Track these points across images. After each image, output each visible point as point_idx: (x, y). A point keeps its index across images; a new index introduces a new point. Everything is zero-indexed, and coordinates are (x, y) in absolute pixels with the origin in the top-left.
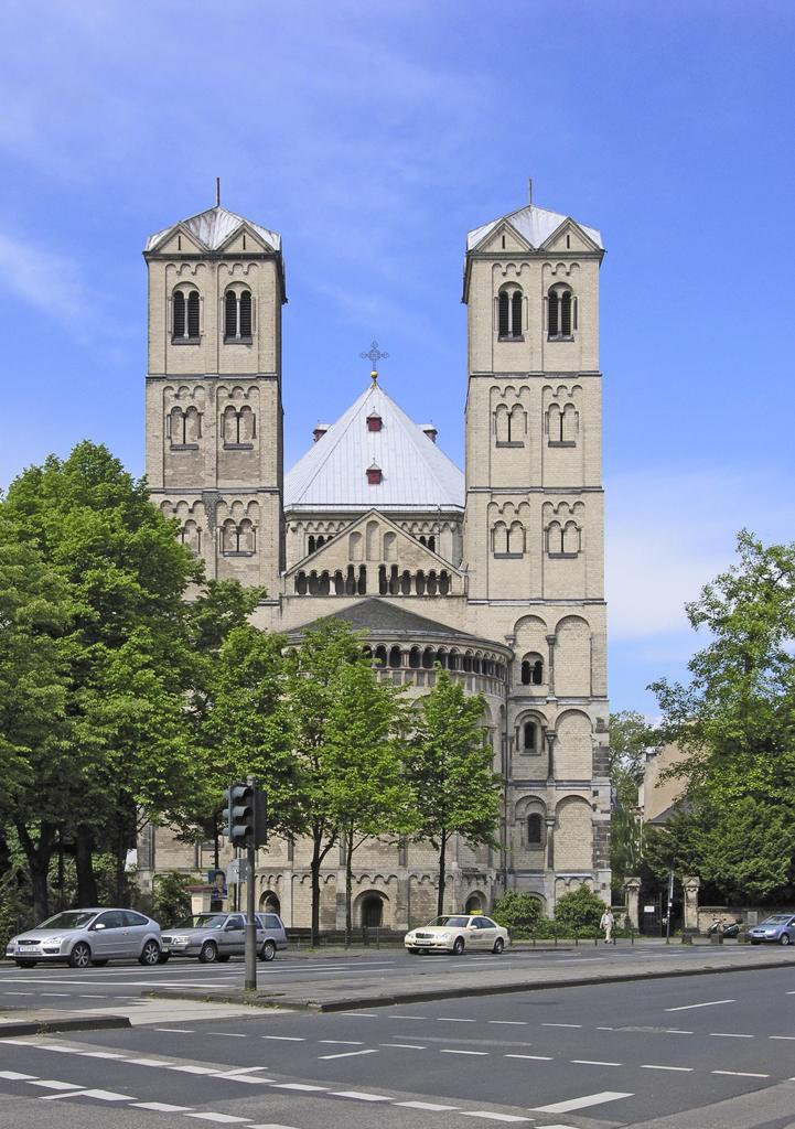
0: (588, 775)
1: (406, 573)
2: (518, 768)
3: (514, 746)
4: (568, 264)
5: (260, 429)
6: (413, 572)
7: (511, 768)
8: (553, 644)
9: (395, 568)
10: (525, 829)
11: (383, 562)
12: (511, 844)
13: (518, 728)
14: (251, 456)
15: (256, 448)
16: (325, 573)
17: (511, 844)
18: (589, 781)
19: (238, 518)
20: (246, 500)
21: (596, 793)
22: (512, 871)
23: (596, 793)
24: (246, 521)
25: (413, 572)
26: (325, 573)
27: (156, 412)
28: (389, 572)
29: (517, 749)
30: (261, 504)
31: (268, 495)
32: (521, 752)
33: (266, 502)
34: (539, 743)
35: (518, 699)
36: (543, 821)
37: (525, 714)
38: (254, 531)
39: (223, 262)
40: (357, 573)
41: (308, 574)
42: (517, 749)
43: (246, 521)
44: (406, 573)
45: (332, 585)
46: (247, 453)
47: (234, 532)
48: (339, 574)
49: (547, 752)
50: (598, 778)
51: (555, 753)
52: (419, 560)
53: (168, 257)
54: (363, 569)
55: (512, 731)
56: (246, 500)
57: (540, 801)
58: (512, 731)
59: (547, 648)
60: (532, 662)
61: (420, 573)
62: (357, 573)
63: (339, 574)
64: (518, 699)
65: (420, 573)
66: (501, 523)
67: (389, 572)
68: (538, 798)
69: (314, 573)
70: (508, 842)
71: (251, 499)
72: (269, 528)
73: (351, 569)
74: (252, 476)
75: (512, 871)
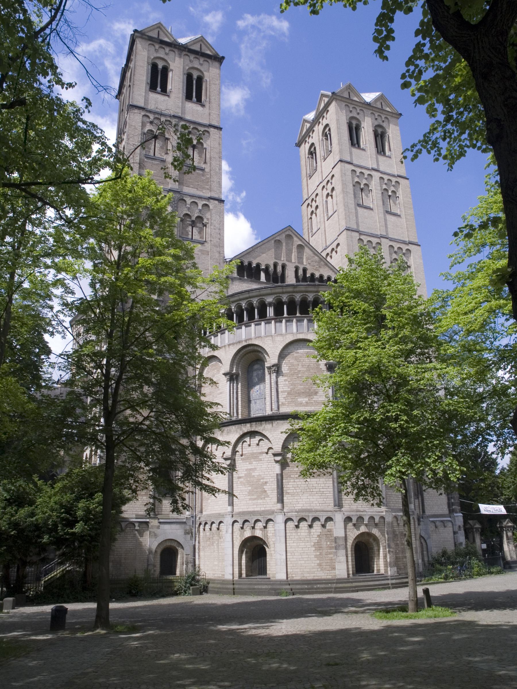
1: (313, 275)
4: (383, 117)
5: (210, 158)
6: (317, 275)
9: (305, 270)
11: (297, 264)
14: (203, 175)
15: (206, 170)
16: (258, 265)
20: (201, 203)
24: (200, 218)
25: (317, 275)
26: (258, 265)
27: (136, 128)
28: (301, 272)
30: (211, 207)
31: (216, 202)
33: (215, 207)
39: (187, 53)
40: (279, 269)
41: (246, 264)
43: (200, 218)
44: (313, 275)
45: (263, 275)
46: (200, 172)
48: (267, 267)
52: (320, 267)
53: (150, 39)
54: (284, 267)
56: (201, 203)
61: (321, 276)
62: (279, 269)
63: (267, 267)
65: (321, 276)
67: (301, 272)
69: (250, 264)
71: (204, 202)
73: (275, 265)
74: (204, 188)
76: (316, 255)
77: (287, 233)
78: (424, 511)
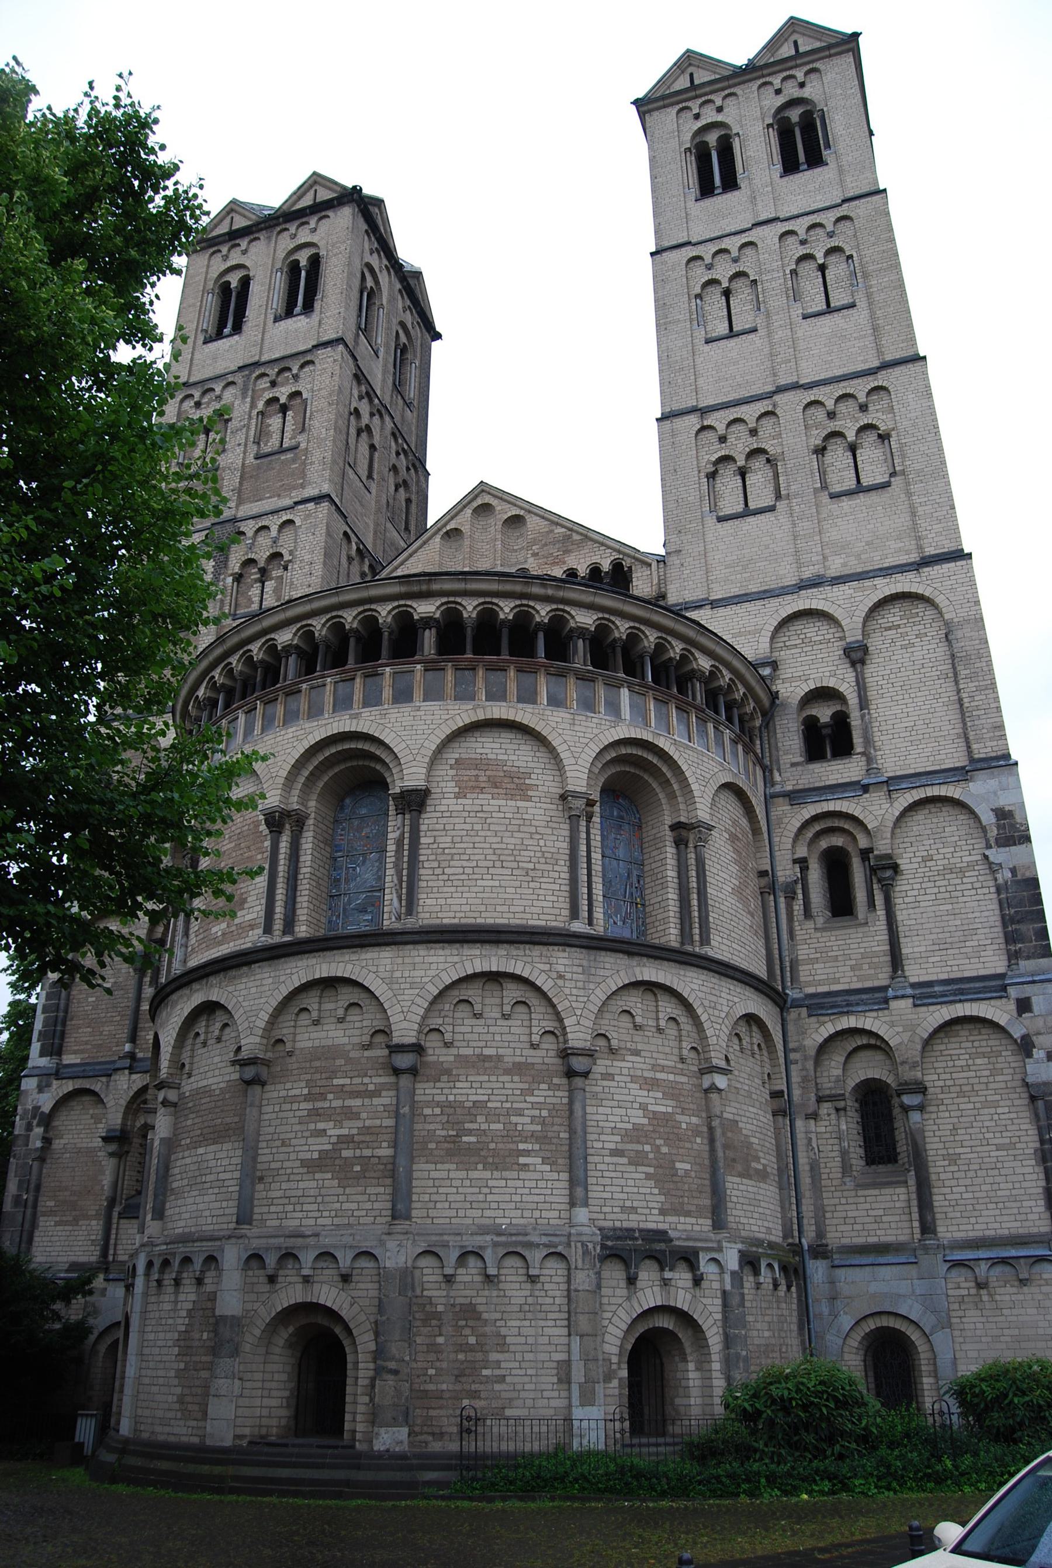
0: (994, 962)
2: (813, 961)
3: (798, 907)
7: (794, 964)
8: (863, 662)
10: (849, 1125)
12: (814, 1167)
13: (802, 863)
17: (814, 1167)
18: (1002, 976)
19: (261, 556)
20: (274, 523)
21: (1024, 1006)
22: (820, 1251)
23: (1024, 1006)
24: (276, 556)
29: (808, 914)
32: (820, 921)
34: (860, 895)
35: (796, 797)
36: (895, 1101)
37: (817, 827)
38: (286, 568)
42: (808, 914)
43: (276, 556)
47: (256, 581)
49: (881, 913)
50: (1025, 965)
51: (901, 916)
55: (786, 872)
56: (274, 523)
57: (876, 1044)
58: (786, 872)
59: (850, 676)
60: (824, 713)
64: (796, 797)
66: (727, 459)
68: (870, 1033)
70: (803, 1160)
72: (307, 557)
75: (820, 1251)
76: (557, 524)
77: (479, 501)
78: (927, 1228)
